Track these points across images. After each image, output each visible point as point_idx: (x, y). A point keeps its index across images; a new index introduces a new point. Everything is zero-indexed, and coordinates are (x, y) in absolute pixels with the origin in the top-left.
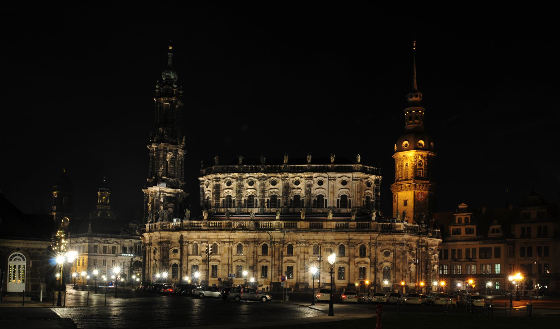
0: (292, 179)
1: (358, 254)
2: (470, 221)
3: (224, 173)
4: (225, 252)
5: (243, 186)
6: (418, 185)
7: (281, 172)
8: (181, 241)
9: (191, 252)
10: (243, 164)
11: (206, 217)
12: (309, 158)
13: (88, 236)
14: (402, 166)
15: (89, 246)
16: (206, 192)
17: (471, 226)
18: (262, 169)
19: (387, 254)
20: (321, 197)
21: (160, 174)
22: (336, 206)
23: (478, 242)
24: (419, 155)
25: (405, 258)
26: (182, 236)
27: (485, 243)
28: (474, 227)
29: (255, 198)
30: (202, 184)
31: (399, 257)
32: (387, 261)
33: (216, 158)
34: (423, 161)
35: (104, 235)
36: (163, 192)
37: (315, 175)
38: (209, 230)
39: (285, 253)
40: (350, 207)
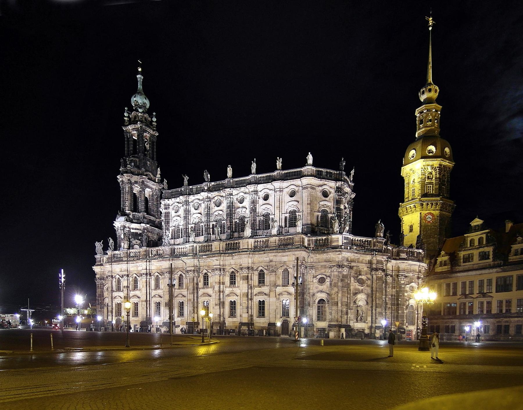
1: (280, 282)
2: (484, 243)
17: (486, 249)
19: (322, 281)
22: (283, 225)
23: (495, 270)
25: (348, 286)
27: (504, 271)
28: (490, 249)
31: (336, 285)
32: (322, 291)
39: (201, 285)
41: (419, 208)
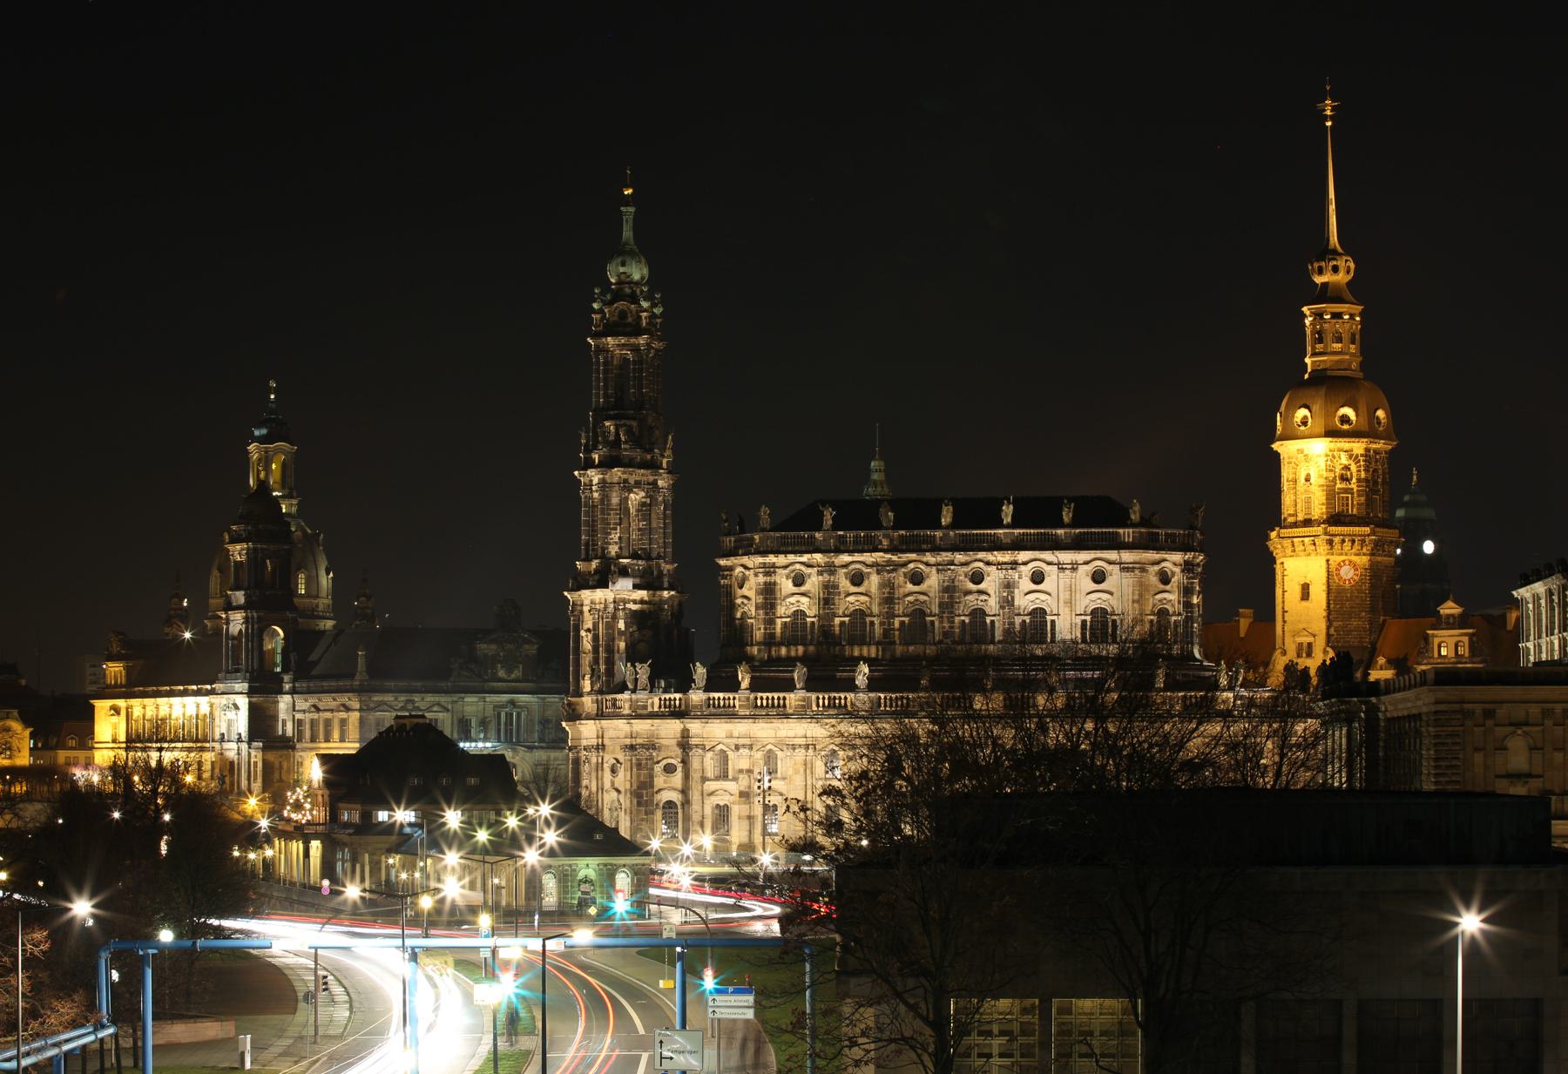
0: (965, 569)
3: (786, 553)
4: (797, 772)
5: (836, 587)
6: (1337, 539)
7: (936, 549)
8: (685, 744)
9: (710, 773)
10: (835, 527)
11: (745, 684)
12: (1008, 512)
13: (360, 691)
14: (1295, 481)
15: (362, 721)
16: (739, 601)
18: (885, 542)
20: (1039, 613)
21: (613, 550)
24: (1340, 450)
26: (685, 734)
29: (868, 619)
30: (724, 577)
33: (764, 512)
34: (1353, 468)
35: (402, 684)
36: (625, 601)
37: (1023, 556)
38: (754, 717)
40: (1114, 641)
41: (1322, 547)
